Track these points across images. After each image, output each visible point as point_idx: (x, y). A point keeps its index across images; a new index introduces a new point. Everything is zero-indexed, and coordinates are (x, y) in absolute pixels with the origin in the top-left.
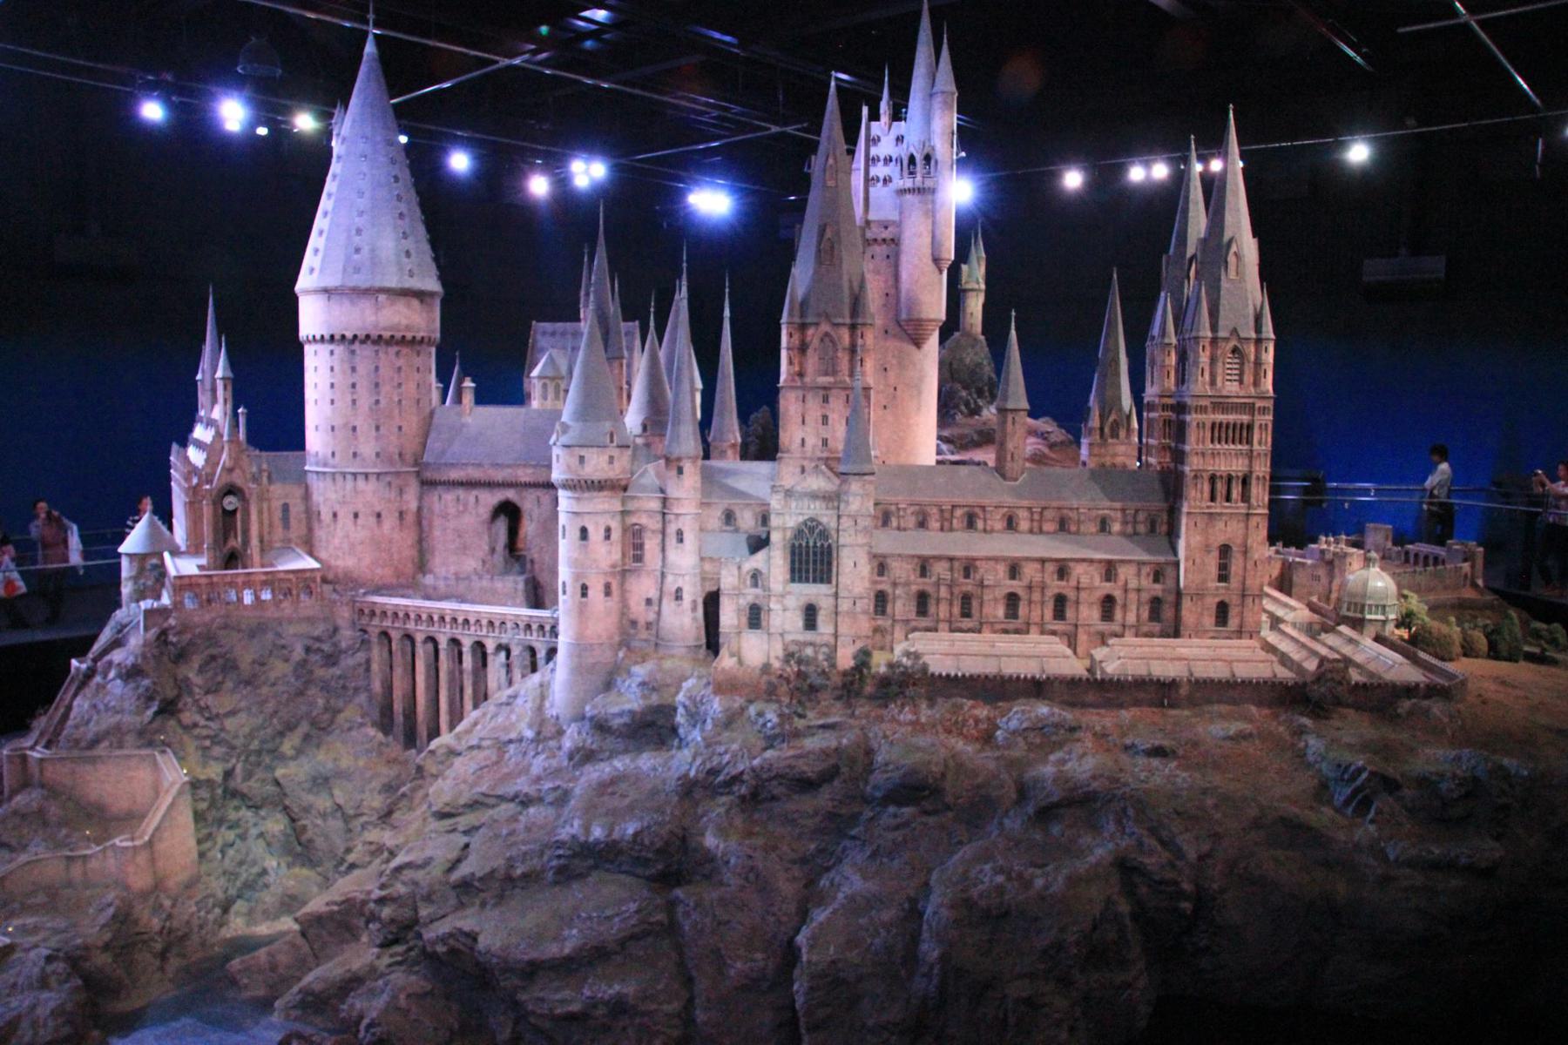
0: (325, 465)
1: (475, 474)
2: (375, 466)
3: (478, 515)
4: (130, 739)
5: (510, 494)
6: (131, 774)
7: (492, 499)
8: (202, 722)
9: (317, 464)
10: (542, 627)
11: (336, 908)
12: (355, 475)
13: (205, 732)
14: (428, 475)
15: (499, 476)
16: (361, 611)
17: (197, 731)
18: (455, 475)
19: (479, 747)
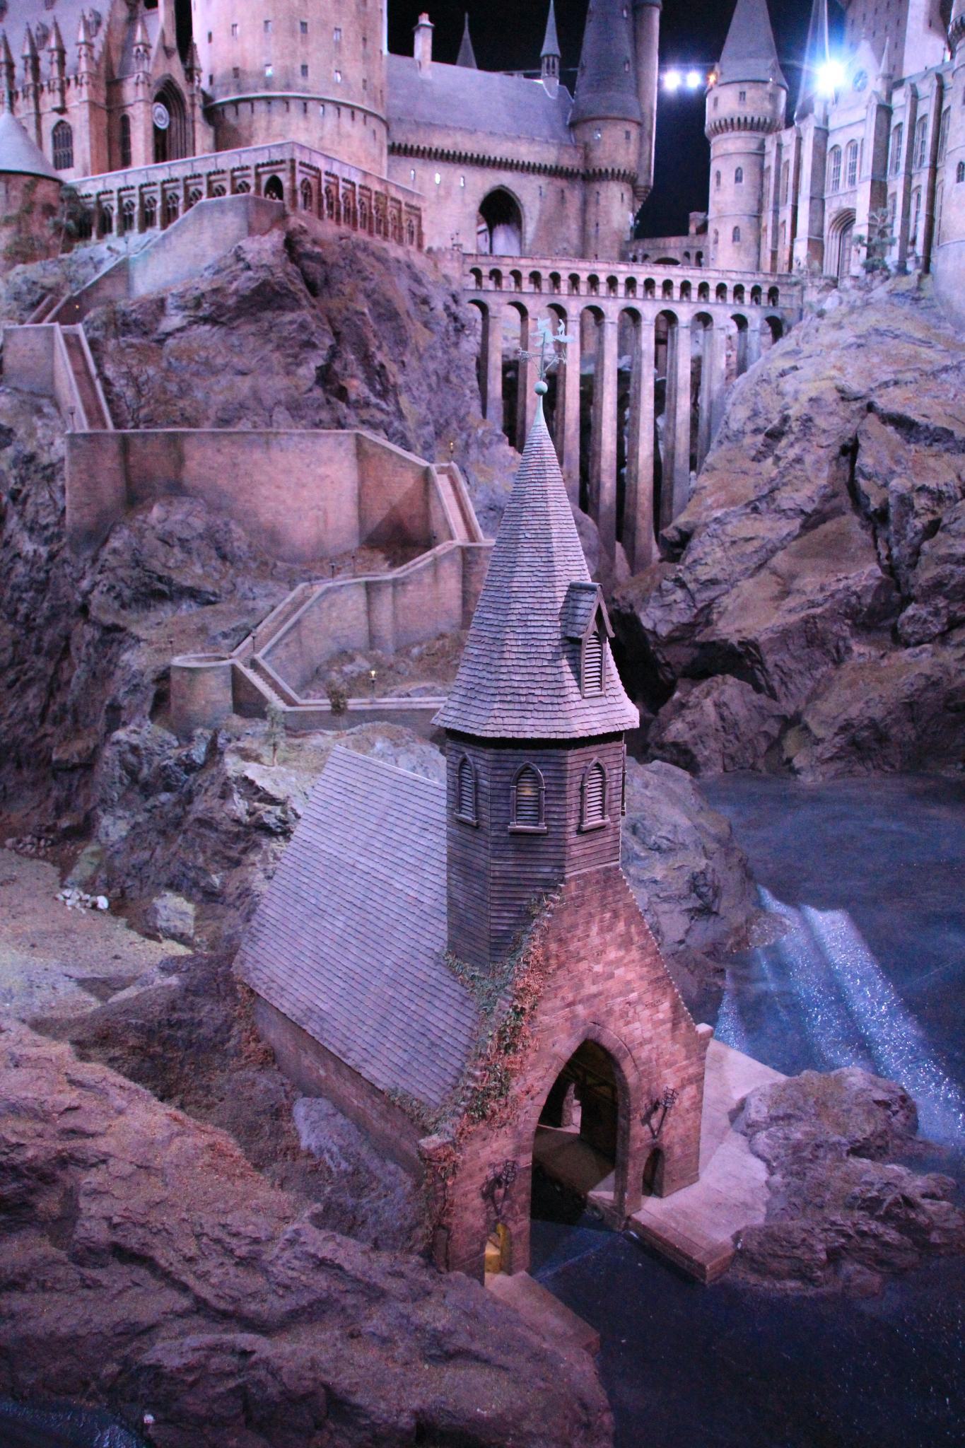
0: (288, 87)
1: (467, 145)
2: (362, 102)
3: (465, 205)
4: (281, 415)
5: (506, 179)
6: (321, 471)
7: (486, 181)
8: (374, 400)
9: (267, 86)
10: (756, 291)
11: (819, 610)
12: (338, 105)
13: (380, 416)
14: (400, 139)
15: (500, 150)
16: (476, 272)
17: (365, 414)
18: (440, 142)
19: (896, 383)
